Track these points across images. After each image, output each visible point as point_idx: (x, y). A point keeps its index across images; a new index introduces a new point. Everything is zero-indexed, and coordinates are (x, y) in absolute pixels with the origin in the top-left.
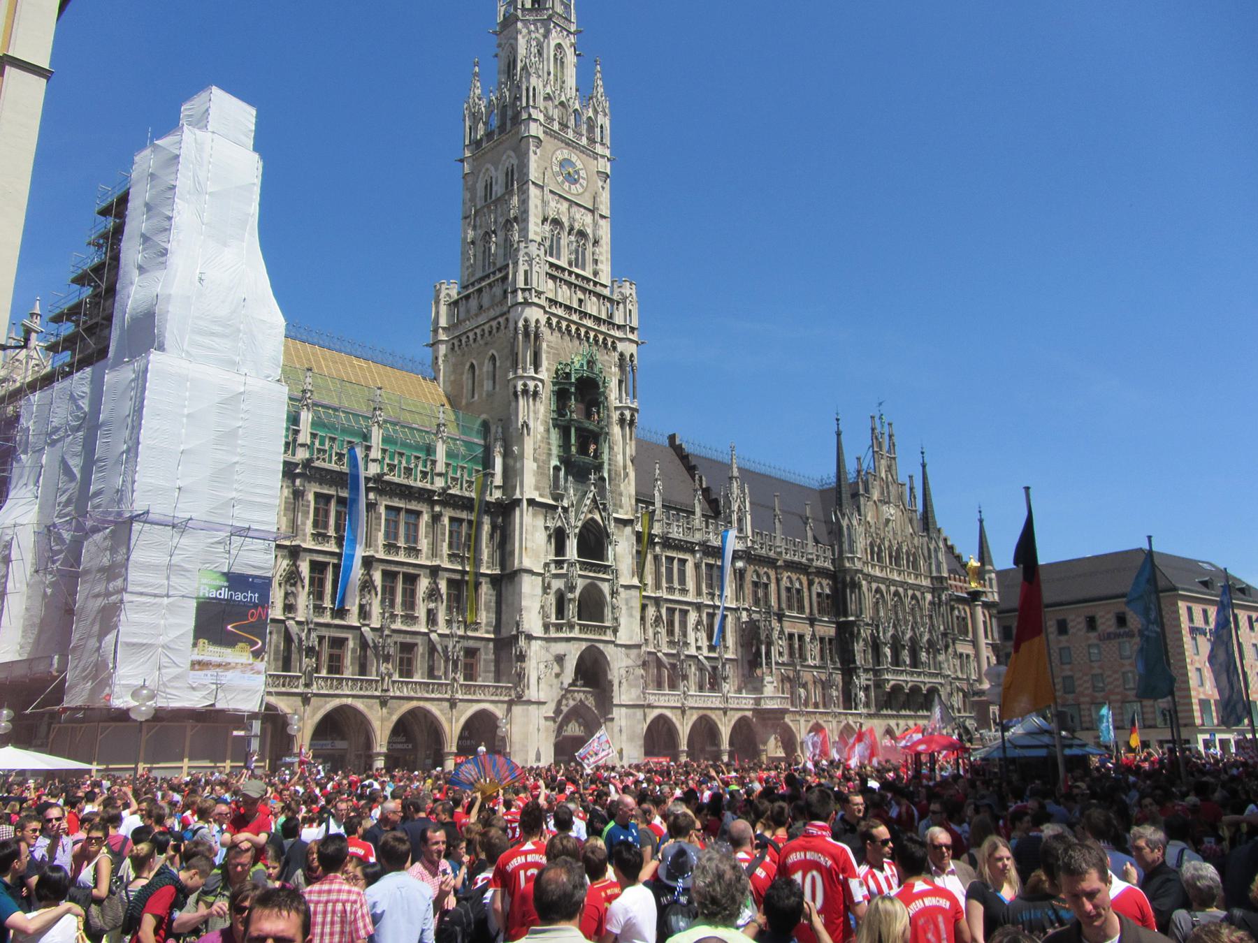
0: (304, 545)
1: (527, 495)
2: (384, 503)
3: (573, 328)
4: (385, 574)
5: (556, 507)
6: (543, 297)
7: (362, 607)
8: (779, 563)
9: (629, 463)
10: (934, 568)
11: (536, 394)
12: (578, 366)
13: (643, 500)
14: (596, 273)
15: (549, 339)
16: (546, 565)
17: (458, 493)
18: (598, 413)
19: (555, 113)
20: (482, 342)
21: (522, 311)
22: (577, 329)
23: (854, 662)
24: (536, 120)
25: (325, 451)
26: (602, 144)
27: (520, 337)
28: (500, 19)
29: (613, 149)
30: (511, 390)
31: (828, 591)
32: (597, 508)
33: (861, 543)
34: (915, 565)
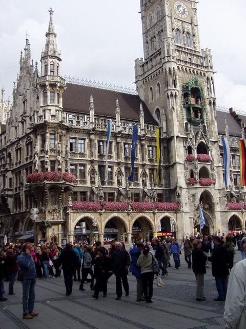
1: (175, 135)
2: (123, 142)
3: (188, 69)
7: (118, 180)
11: (176, 96)
13: (221, 133)
15: (179, 75)
17: (150, 136)
27: (168, 75)
30: (166, 95)
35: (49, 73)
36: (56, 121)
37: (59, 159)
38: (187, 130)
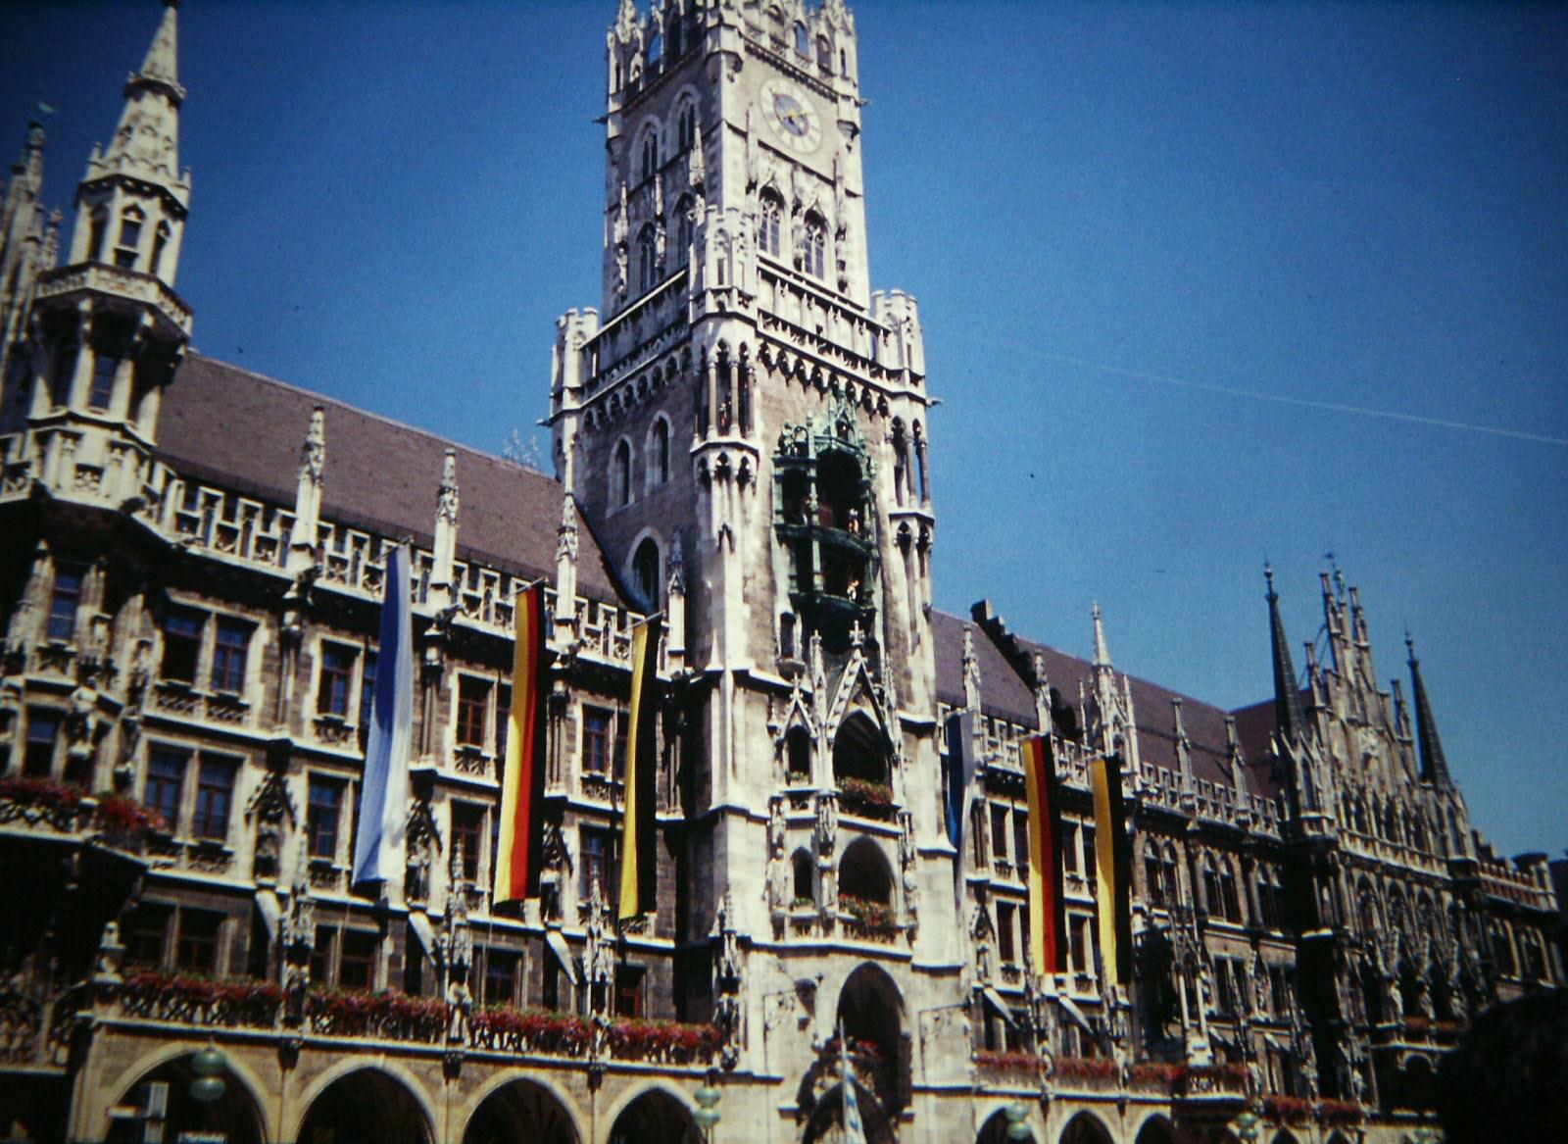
4: (457, 808)
5: (791, 690)
7: (411, 873)
8: (1190, 827)
10: (1451, 844)
11: (744, 477)
12: (820, 434)
14: (842, 285)
15: (765, 384)
16: (775, 801)
18: (861, 518)
21: (717, 327)
23: (1337, 1013)
24: (731, 27)
25: (344, 563)
26: (845, 78)
29: (863, 85)
30: (697, 471)
31: (1276, 883)
32: (866, 691)
33: (1329, 797)
34: (1421, 842)
37: (84, 706)
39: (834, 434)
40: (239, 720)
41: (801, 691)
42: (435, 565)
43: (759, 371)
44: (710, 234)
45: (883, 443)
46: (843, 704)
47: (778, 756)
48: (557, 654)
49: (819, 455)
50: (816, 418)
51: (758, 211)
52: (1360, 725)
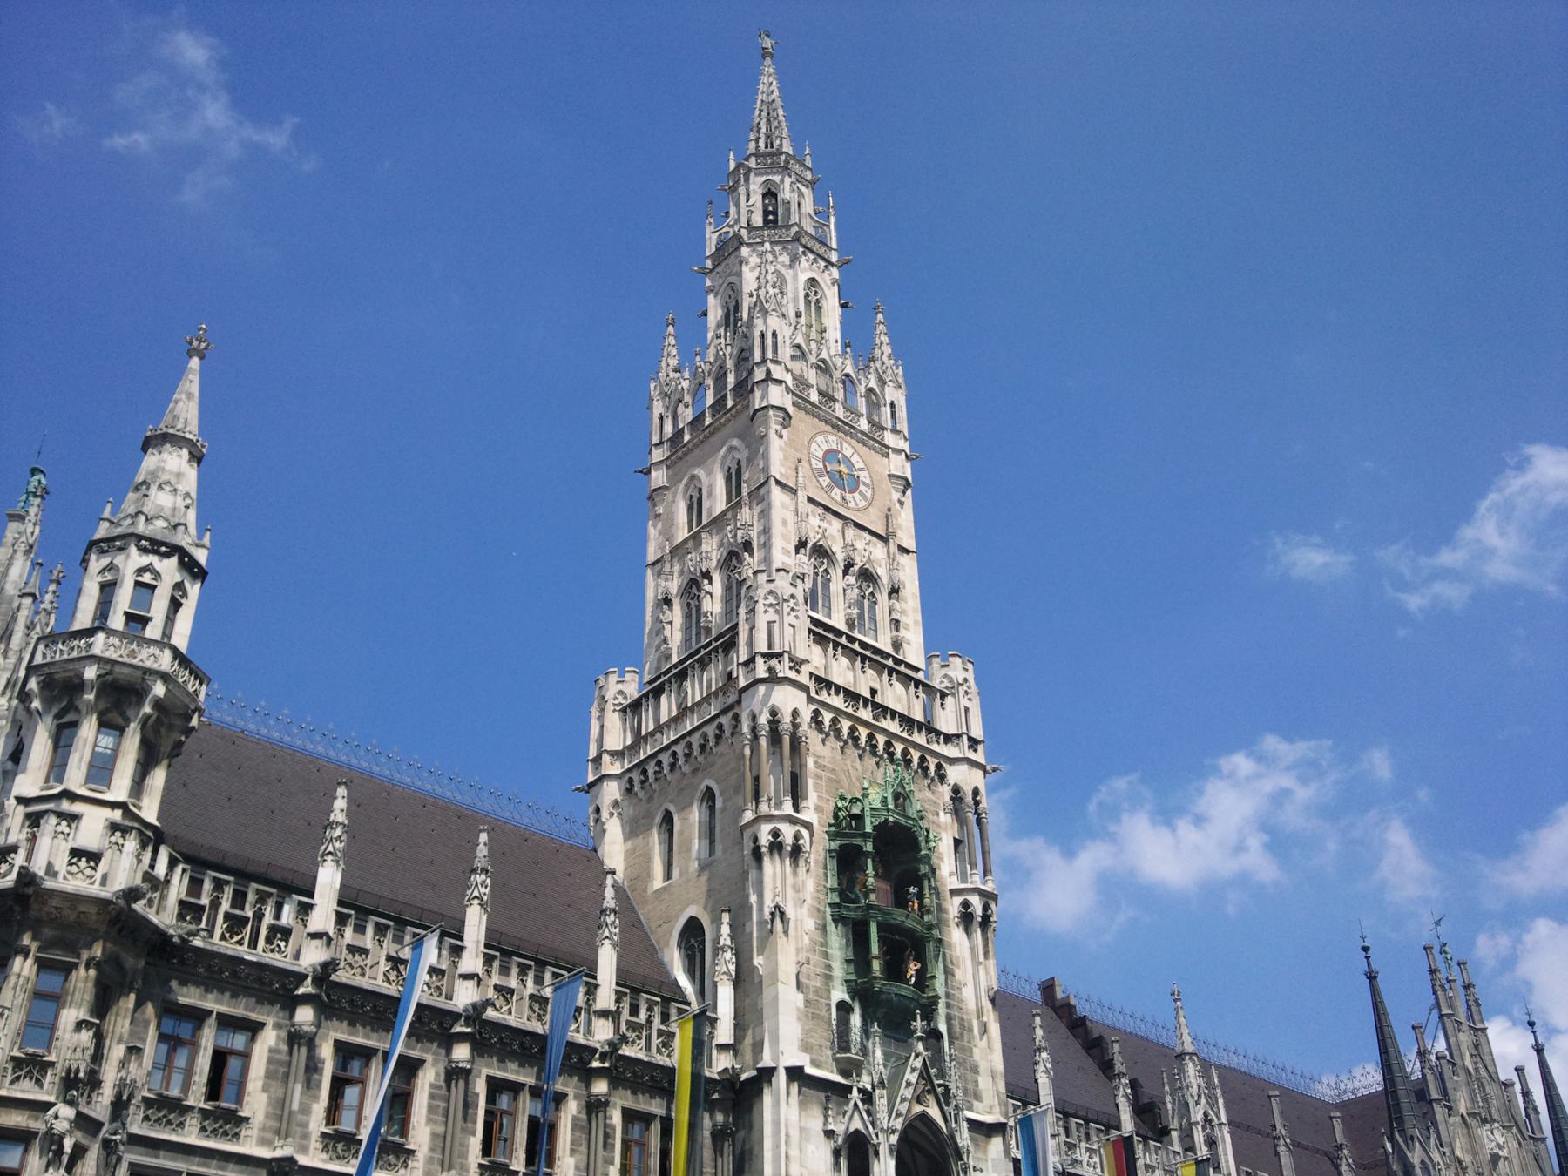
0: (303, 1160)
2: (485, 1071)
3: (863, 733)
5: (849, 1089)
6: (805, 669)
9: (988, 1005)
11: (796, 851)
14: (897, 645)
15: (819, 752)
17: (642, 1056)
18: (920, 896)
19: (812, 376)
20: (686, 769)
21: (768, 695)
22: (871, 737)
26: (895, 431)
27: (763, 742)
28: (710, 249)
32: (933, 1091)
35: (117, 621)
36: (95, 890)
37: (61, 1126)
38: (843, 1041)
39: (891, 806)
40: (237, 1135)
41: (860, 1090)
42: (465, 954)
43: (812, 739)
44: (760, 594)
45: (941, 813)
46: (906, 1104)
47: (837, 1164)
48: (596, 1050)
49: (875, 828)
50: (871, 785)
51: (809, 570)
52: (1484, 1121)
